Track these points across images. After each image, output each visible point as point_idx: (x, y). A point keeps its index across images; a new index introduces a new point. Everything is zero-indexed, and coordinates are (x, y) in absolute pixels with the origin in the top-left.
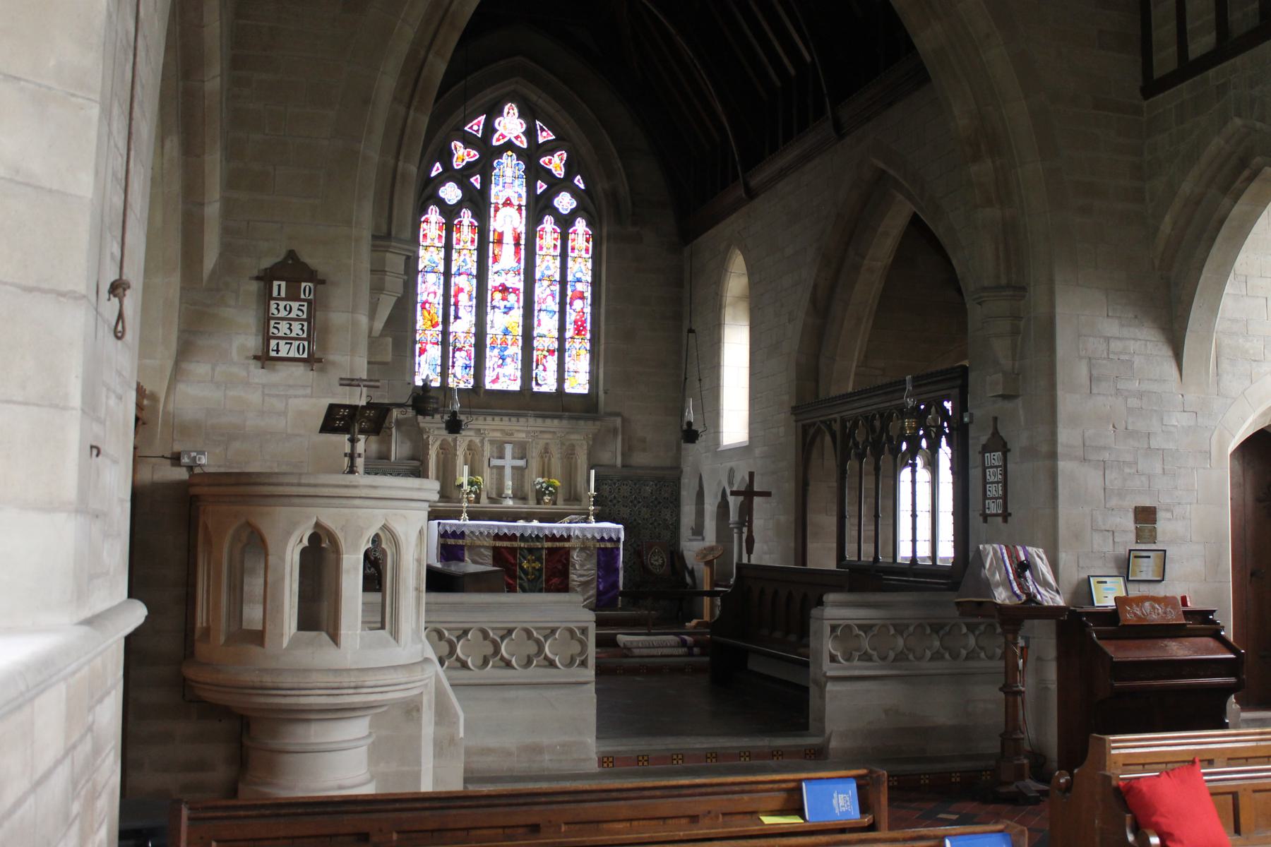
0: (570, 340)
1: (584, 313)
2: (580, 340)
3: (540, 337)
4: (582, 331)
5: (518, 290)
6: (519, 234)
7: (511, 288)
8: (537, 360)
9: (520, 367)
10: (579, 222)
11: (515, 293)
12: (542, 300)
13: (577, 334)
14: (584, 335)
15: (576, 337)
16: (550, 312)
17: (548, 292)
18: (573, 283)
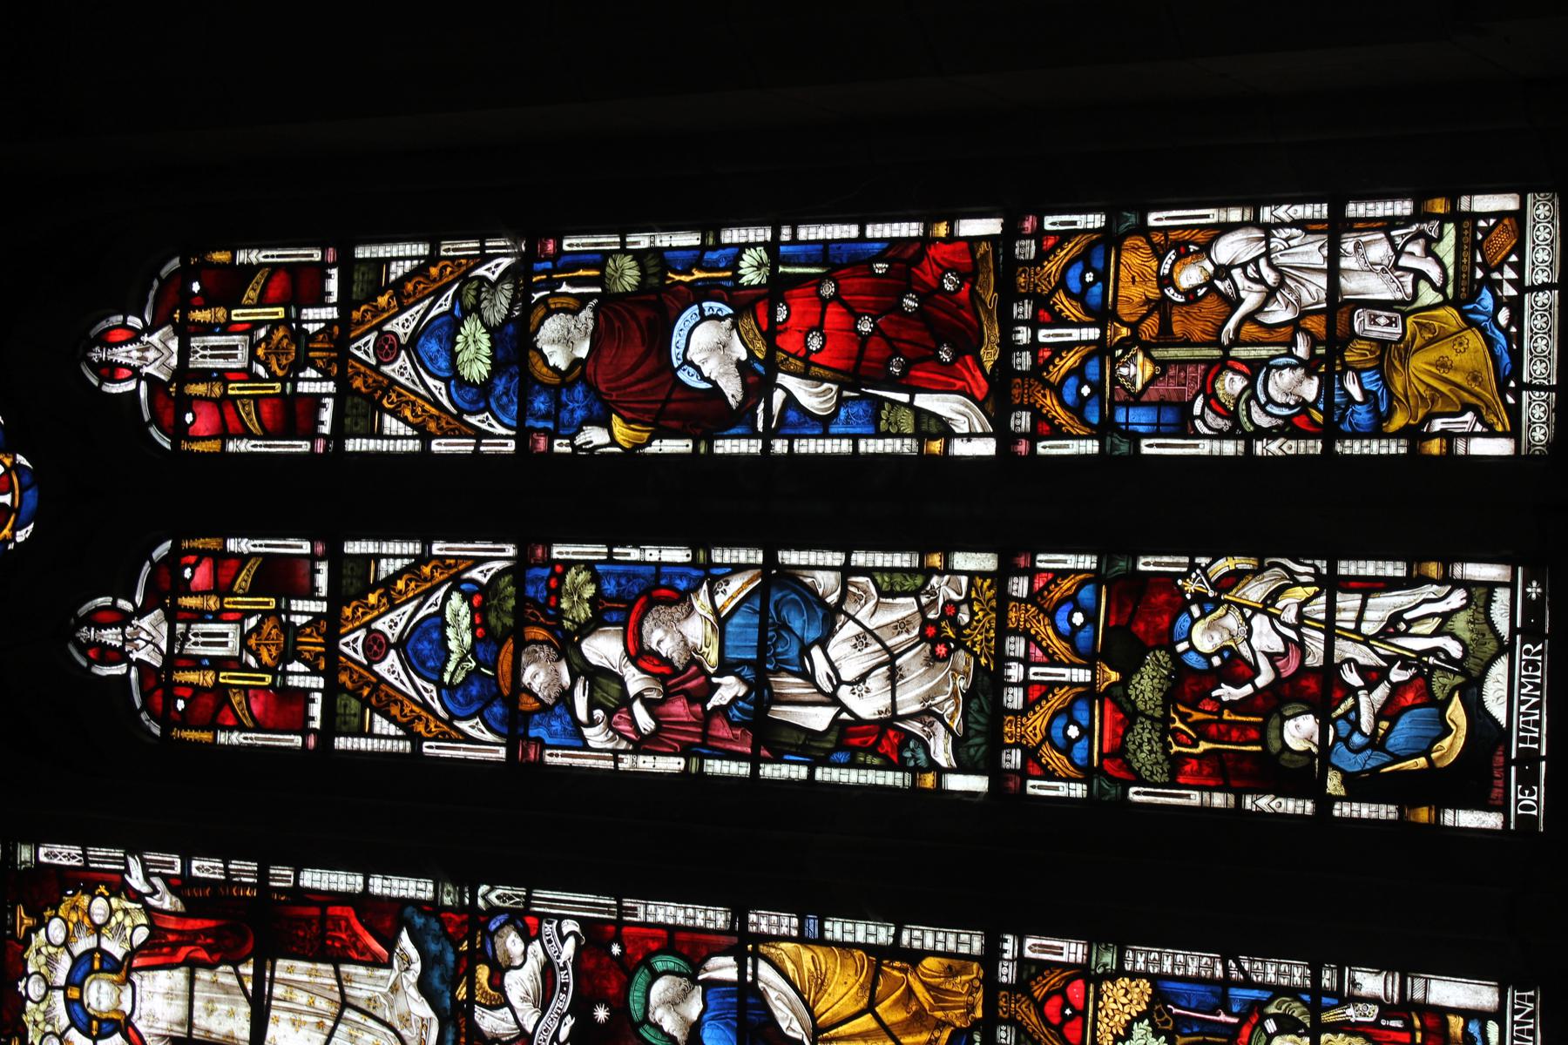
0: (1022, 421)
1: (777, 288)
2: (1024, 310)
3: (997, 745)
4: (927, 295)
5: (593, 935)
6: (193, 908)
7: (581, 1009)
8: (1221, 771)
9: (1298, 974)
10: (110, 371)
11: (626, 969)
12: (679, 708)
13: (969, 344)
14: (969, 275)
15: (989, 357)
16: (770, 629)
17: (604, 649)
18: (540, 404)
